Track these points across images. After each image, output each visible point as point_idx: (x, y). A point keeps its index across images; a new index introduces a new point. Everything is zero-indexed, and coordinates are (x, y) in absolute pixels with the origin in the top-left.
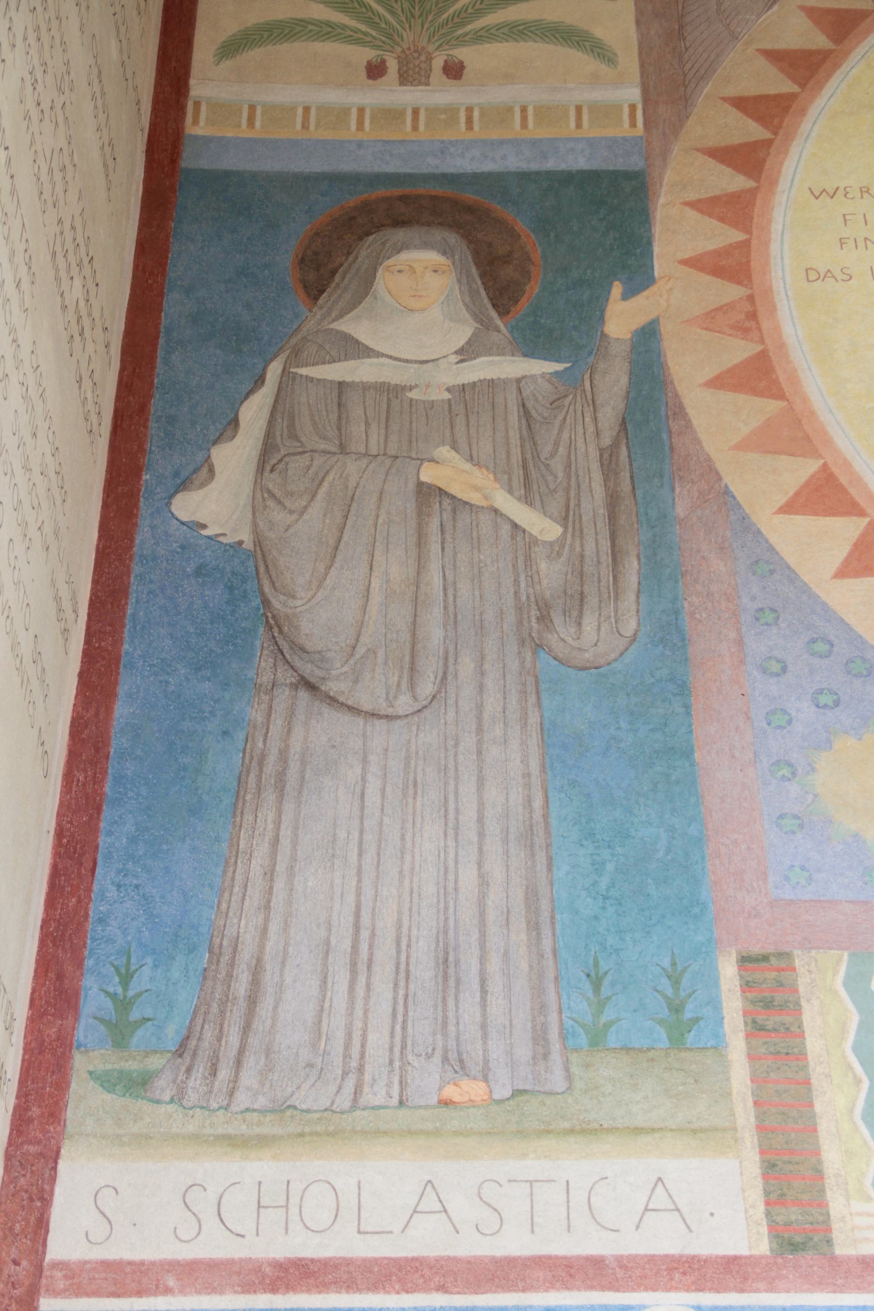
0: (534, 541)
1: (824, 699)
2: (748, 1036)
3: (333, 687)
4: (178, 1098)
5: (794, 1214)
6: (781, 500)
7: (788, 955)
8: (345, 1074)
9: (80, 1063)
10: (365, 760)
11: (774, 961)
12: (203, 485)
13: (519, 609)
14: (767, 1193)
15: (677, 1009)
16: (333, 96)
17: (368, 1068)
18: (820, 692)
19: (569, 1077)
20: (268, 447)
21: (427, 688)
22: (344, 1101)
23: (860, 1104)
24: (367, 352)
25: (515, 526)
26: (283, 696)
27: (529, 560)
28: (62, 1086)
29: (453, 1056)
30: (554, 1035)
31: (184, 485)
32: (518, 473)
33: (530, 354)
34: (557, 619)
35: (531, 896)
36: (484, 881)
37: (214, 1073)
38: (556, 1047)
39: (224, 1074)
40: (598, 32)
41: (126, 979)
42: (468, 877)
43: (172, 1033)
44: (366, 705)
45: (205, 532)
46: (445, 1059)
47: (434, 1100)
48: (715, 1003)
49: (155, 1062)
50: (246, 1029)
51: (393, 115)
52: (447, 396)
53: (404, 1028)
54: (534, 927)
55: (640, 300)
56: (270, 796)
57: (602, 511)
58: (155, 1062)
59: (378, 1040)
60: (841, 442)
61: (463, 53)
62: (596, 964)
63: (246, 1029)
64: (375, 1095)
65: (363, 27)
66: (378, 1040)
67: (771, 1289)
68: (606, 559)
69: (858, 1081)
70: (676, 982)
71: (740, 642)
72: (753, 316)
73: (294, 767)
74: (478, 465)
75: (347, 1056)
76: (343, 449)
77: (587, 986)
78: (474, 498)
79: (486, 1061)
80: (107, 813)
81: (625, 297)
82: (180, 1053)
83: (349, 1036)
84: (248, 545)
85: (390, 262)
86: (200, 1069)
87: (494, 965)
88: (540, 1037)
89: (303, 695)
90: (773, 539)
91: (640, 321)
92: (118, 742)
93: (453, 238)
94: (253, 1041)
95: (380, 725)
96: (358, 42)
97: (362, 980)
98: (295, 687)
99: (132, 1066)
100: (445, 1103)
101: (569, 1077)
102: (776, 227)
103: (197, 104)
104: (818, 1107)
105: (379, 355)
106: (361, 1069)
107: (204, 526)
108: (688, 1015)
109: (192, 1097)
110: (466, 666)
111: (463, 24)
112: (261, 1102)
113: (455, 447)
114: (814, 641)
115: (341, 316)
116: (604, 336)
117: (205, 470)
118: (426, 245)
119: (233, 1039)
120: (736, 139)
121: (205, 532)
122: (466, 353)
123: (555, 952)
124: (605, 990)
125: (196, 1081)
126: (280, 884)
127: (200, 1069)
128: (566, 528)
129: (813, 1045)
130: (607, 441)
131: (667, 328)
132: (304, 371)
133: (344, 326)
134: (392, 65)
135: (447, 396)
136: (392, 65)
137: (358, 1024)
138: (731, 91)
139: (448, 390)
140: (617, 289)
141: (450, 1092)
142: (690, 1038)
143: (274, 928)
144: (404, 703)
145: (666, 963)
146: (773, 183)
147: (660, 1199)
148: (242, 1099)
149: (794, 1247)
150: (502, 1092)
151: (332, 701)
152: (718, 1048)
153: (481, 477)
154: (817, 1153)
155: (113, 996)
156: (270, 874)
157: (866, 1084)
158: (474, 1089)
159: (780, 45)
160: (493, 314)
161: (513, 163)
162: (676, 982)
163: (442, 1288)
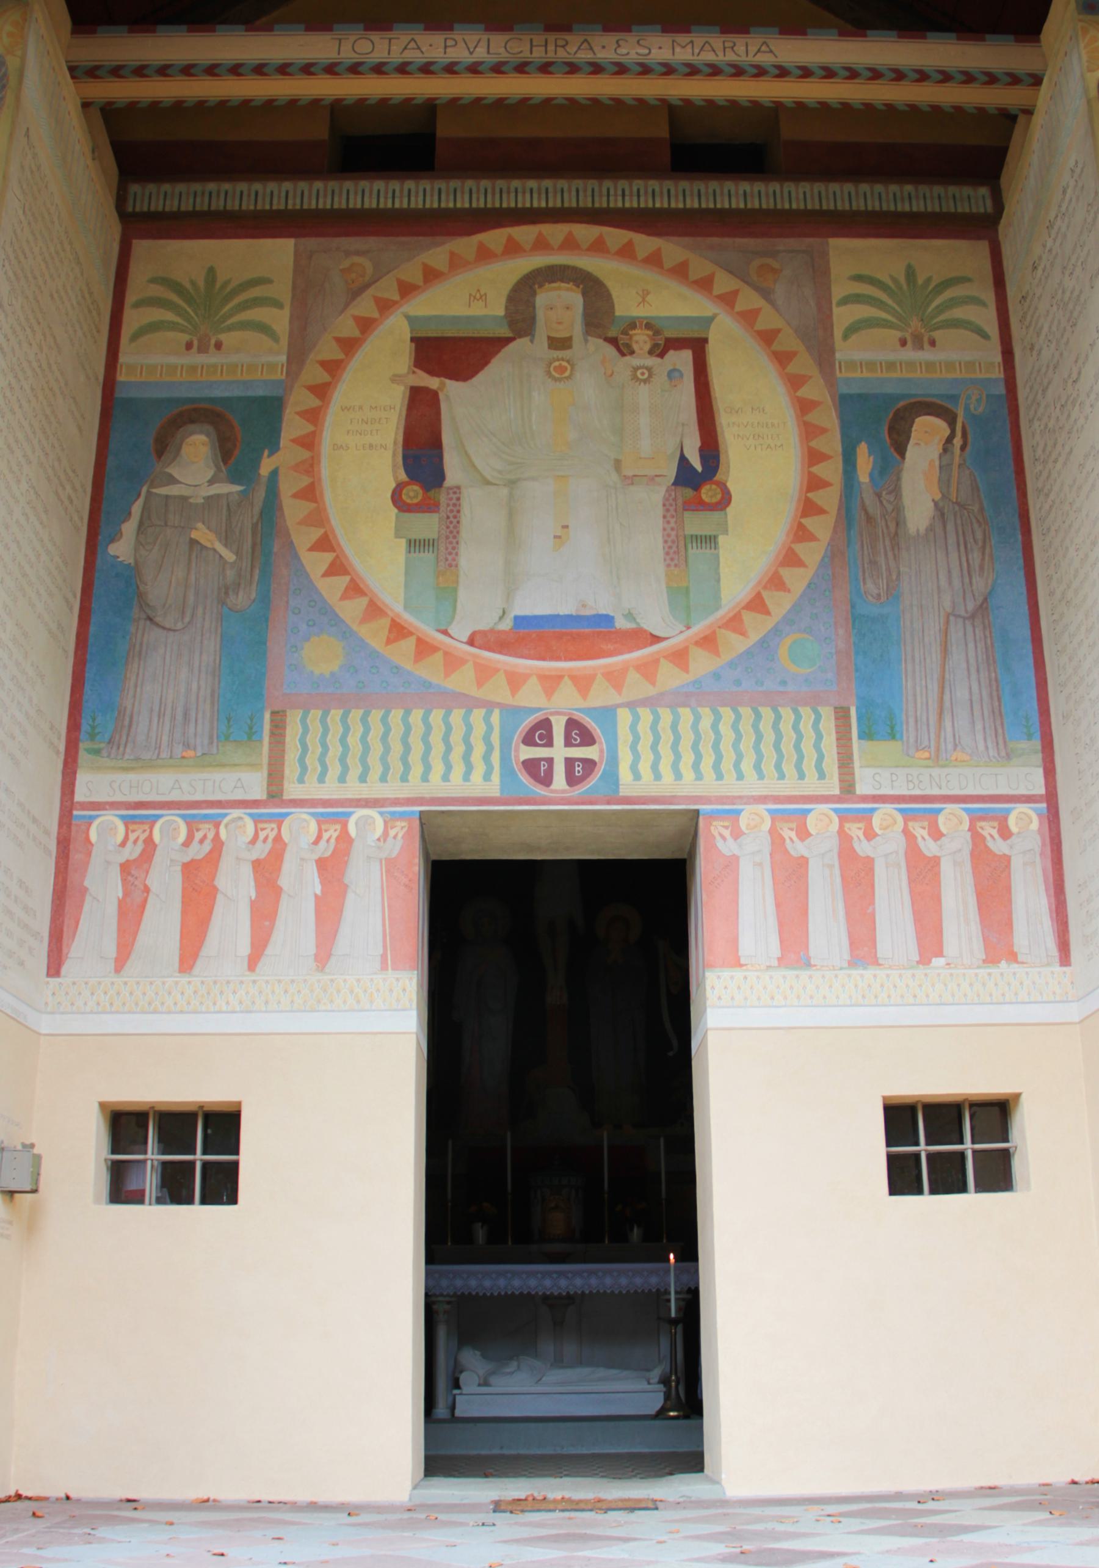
0: (226, 562)
1: (311, 623)
2: (270, 736)
3: (158, 619)
4: (109, 756)
5: (274, 788)
6: (309, 546)
7: (285, 711)
8: (155, 749)
9: (82, 746)
10: (166, 646)
11: (281, 713)
12: (119, 540)
13: (219, 589)
14: (268, 782)
15: (251, 728)
16: (173, 360)
17: (162, 747)
18: (309, 621)
19: (218, 749)
20: (141, 524)
21: (187, 620)
22: (155, 757)
23: (297, 758)
24: (178, 482)
25: (221, 556)
26: (142, 623)
27: (224, 570)
28: (77, 752)
29: (186, 743)
30: (215, 737)
31: (112, 541)
32: (224, 534)
33: (232, 483)
34: (231, 593)
35: (213, 691)
36: (199, 688)
37: (118, 748)
38: (215, 740)
39: (121, 749)
40: (275, 327)
41: (94, 720)
42: (195, 686)
43: (107, 737)
44: (168, 626)
45: (119, 560)
46: (184, 745)
47: (179, 756)
48: (262, 727)
49: (102, 745)
50: (128, 735)
51: (193, 369)
52: (202, 501)
53: (173, 735)
54: (213, 703)
55: (274, 458)
56: (136, 659)
57: (250, 550)
58: (102, 745)
59: (165, 738)
60: (333, 522)
61: (223, 337)
62: (230, 714)
63: (128, 735)
64: (163, 755)
65: (186, 324)
66: (165, 738)
67: (265, 808)
68: (249, 569)
69: (298, 750)
70: (252, 720)
71: (287, 602)
72: (312, 466)
73: (144, 648)
74: (210, 531)
75: (156, 743)
76: (166, 525)
77: (226, 722)
78: (209, 545)
79: (195, 746)
80: (88, 665)
81: (269, 456)
82: (110, 742)
83: (157, 737)
84: (133, 564)
85: (187, 440)
86: (115, 748)
87: (200, 715)
88: (211, 738)
89: (148, 622)
90: (304, 561)
91: (272, 467)
92: (91, 640)
93: (210, 428)
94: (130, 739)
95: (171, 633)
96: (182, 331)
97: (161, 720)
98: (145, 619)
99: (96, 746)
100: (183, 757)
101: (218, 749)
102: (327, 424)
103: (121, 366)
104: (286, 758)
105: (180, 483)
106: (160, 747)
107: (118, 557)
108: (254, 730)
109: (112, 756)
110: (200, 611)
111: (224, 322)
112: (132, 757)
113: (204, 523)
114: (310, 601)
115: (169, 464)
116: (259, 474)
117: (119, 535)
118: (201, 432)
119: (124, 738)
120: (319, 381)
121: (119, 560)
122: (211, 482)
123: (218, 711)
124: (231, 723)
125: (114, 751)
126: (139, 689)
127: (115, 748)
128: (237, 556)
129: (288, 739)
130: (255, 520)
131: (282, 471)
132: (154, 490)
133: (169, 470)
134: (196, 343)
135: (202, 501)
136: (196, 343)
137: (160, 734)
138: (320, 357)
139: (204, 498)
140: (266, 453)
141: (185, 754)
142: (254, 737)
143: (137, 704)
144: (179, 625)
145: (250, 714)
146: (329, 403)
147: (239, 785)
148: (127, 757)
149: (273, 797)
150: (199, 754)
151: (158, 625)
152: (261, 741)
153: (211, 536)
154: (283, 771)
155: (90, 725)
156: (136, 686)
157: (300, 750)
158: (191, 753)
159: (341, 335)
160: (222, 464)
161: (237, 392)
162: (252, 720)
163: (179, 809)
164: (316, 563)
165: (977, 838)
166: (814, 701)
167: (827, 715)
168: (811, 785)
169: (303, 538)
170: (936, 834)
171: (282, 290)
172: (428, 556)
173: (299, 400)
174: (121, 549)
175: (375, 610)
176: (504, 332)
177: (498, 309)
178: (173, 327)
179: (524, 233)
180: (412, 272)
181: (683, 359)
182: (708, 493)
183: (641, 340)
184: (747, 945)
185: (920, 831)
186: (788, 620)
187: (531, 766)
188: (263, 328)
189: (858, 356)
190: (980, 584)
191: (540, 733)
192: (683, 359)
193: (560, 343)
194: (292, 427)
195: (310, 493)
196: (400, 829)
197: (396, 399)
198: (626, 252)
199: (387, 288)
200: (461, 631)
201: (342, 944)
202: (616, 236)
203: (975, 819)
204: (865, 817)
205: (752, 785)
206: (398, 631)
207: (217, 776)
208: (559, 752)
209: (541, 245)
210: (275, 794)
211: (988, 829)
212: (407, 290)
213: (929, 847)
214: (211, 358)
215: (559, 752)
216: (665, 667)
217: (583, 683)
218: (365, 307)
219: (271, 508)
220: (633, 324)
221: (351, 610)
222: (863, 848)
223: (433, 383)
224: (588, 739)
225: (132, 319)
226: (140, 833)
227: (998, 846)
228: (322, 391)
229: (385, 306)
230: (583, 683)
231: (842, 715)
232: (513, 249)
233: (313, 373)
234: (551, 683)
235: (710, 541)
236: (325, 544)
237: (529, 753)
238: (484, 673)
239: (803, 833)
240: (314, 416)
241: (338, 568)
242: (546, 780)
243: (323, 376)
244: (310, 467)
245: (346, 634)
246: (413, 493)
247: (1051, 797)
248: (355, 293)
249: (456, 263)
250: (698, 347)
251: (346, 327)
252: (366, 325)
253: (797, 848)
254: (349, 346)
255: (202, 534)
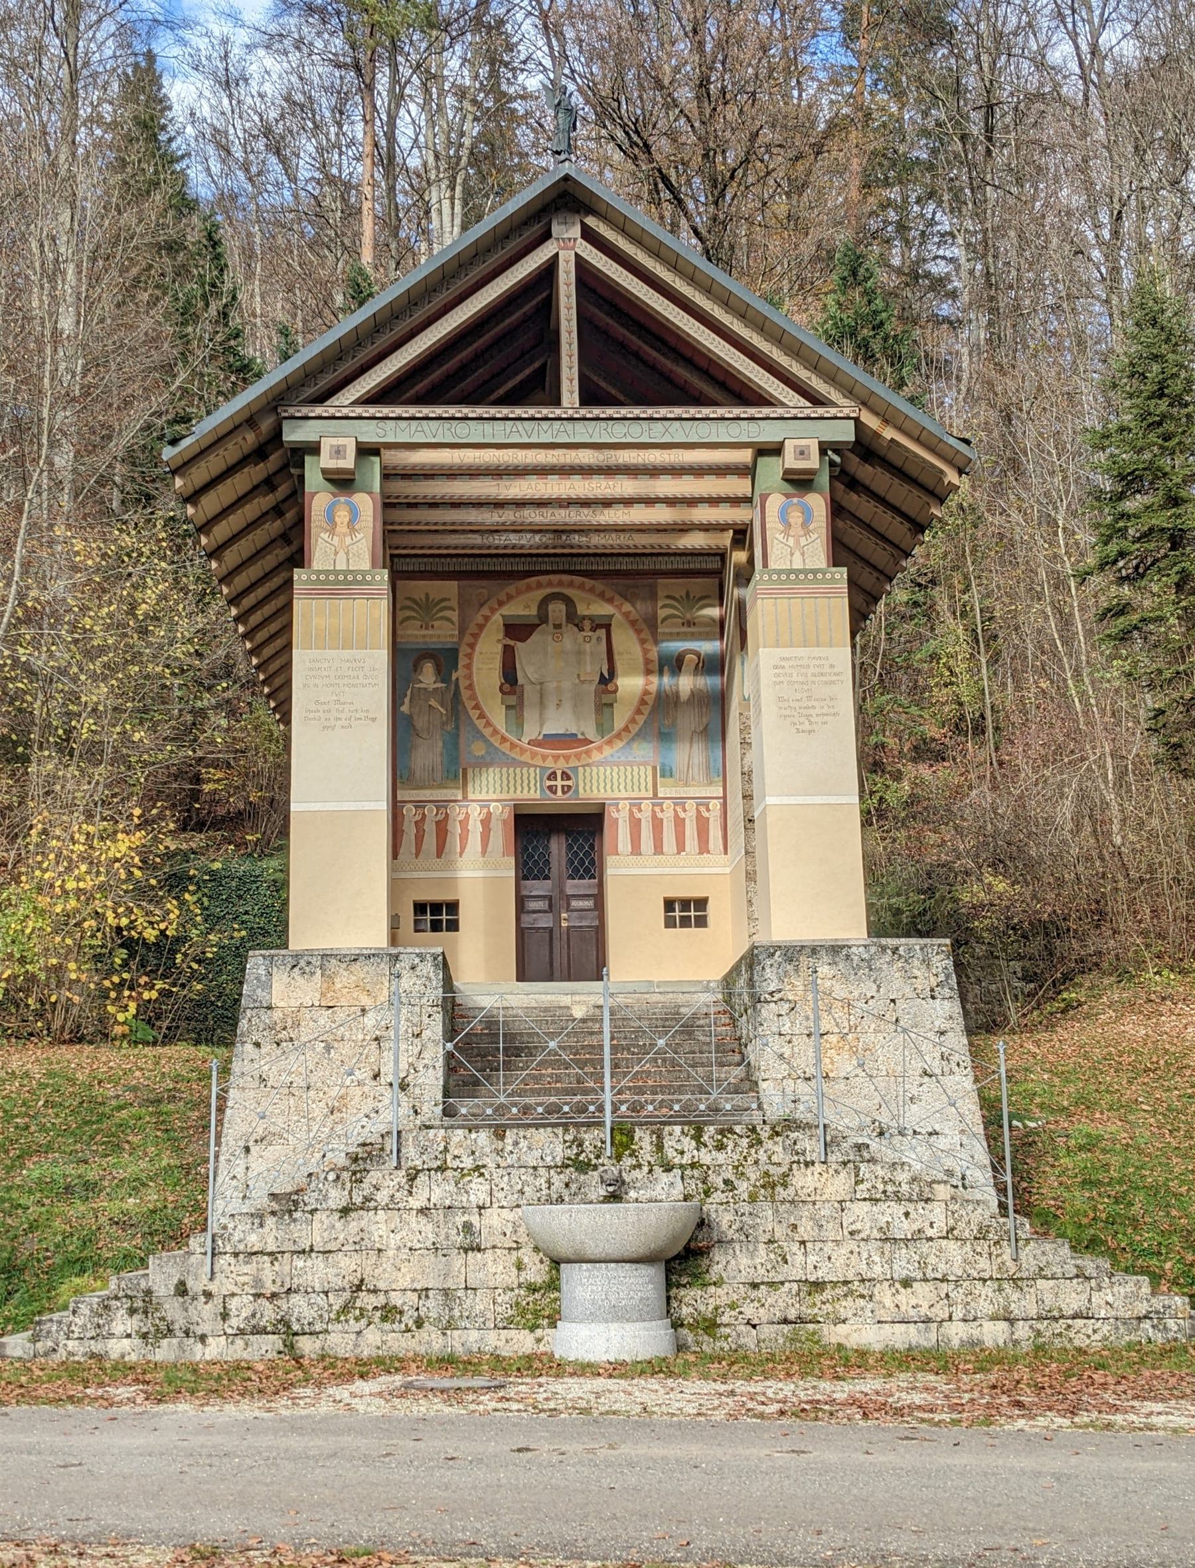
164: (474, 714)
165: (698, 812)
166: (645, 764)
167: (649, 769)
168: (643, 794)
169: (469, 705)
170: (685, 810)
171: (454, 603)
172: (513, 712)
173: (464, 650)
174: (405, 708)
175: (496, 732)
176: (537, 621)
177: (534, 612)
178: (414, 618)
179: (543, 579)
180: (503, 597)
181: (602, 633)
182: (610, 687)
183: (587, 624)
184: (620, 848)
185: (679, 809)
186: (637, 735)
187: (550, 788)
188: (448, 619)
189: (667, 630)
190: (705, 720)
191: (552, 777)
192: (602, 633)
193: (558, 626)
194: (462, 661)
195: (470, 687)
196: (507, 810)
197: (500, 648)
198: (581, 587)
199: (493, 603)
200: (525, 740)
201: (489, 849)
202: (578, 579)
203: (698, 805)
204: (661, 805)
205: (624, 794)
206: (504, 739)
207: (445, 791)
208: (559, 783)
209: (550, 584)
210: (465, 798)
211: (702, 809)
212: (501, 604)
213: (682, 815)
214: (430, 632)
215: (559, 783)
216: (595, 752)
217: (567, 758)
218: (485, 611)
219: (457, 693)
220: (584, 618)
221: (487, 732)
222: (660, 815)
223: (511, 643)
224: (569, 778)
225: (401, 615)
226: (420, 811)
227: (706, 814)
228: (472, 646)
229: (493, 611)
230: (567, 758)
231: (654, 768)
232: (539, 586)
233: (468, 639)
234: (556, 758)
235: (611, 705)
236: (477, 707)
237: (549, 783)
238: (534, 755)
239: (640, 810)
240: (470, 656)
241: (482, 716)
242: (555, 793)
243: (472, 640)
244: (469, 677)
245: (486, 741)
246: (507, 687)
247: (725, 797)
248: (482, 605)
249: (519, 592)
250: (608, 628)
251: (479, 619)
252: (487, 619)
253: (638, 815)
254: (481, 627)
255: (433, 702)
